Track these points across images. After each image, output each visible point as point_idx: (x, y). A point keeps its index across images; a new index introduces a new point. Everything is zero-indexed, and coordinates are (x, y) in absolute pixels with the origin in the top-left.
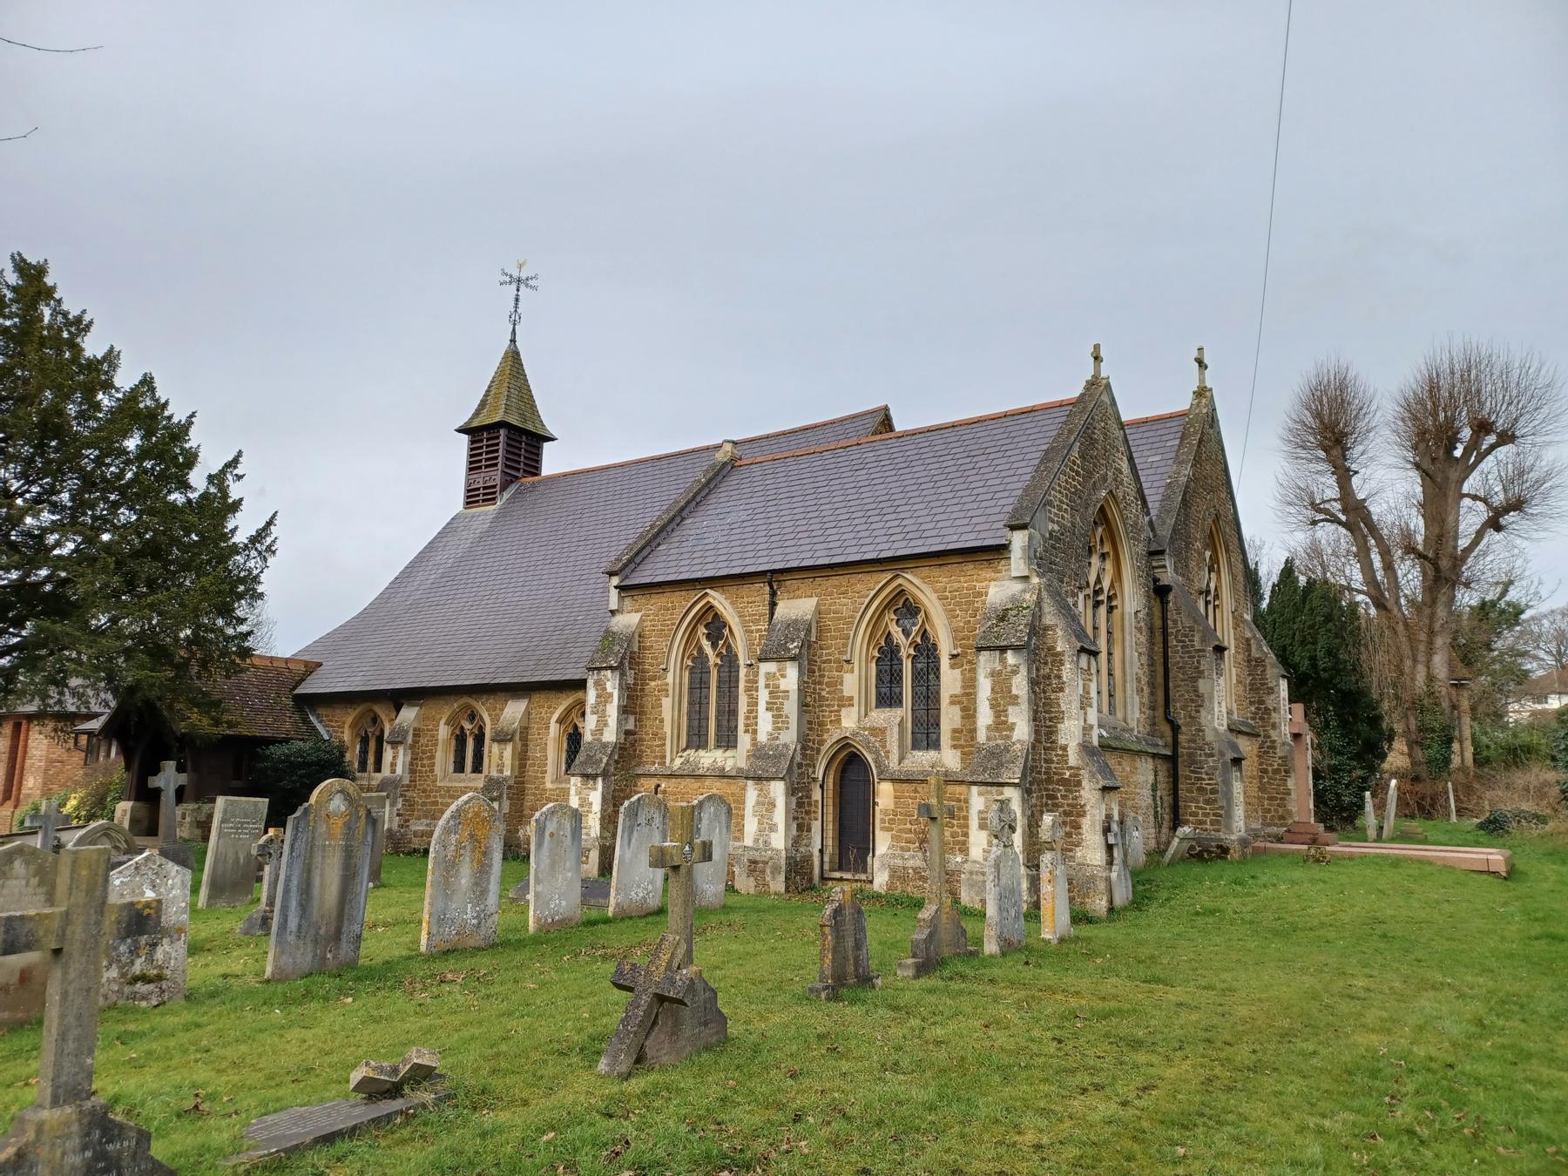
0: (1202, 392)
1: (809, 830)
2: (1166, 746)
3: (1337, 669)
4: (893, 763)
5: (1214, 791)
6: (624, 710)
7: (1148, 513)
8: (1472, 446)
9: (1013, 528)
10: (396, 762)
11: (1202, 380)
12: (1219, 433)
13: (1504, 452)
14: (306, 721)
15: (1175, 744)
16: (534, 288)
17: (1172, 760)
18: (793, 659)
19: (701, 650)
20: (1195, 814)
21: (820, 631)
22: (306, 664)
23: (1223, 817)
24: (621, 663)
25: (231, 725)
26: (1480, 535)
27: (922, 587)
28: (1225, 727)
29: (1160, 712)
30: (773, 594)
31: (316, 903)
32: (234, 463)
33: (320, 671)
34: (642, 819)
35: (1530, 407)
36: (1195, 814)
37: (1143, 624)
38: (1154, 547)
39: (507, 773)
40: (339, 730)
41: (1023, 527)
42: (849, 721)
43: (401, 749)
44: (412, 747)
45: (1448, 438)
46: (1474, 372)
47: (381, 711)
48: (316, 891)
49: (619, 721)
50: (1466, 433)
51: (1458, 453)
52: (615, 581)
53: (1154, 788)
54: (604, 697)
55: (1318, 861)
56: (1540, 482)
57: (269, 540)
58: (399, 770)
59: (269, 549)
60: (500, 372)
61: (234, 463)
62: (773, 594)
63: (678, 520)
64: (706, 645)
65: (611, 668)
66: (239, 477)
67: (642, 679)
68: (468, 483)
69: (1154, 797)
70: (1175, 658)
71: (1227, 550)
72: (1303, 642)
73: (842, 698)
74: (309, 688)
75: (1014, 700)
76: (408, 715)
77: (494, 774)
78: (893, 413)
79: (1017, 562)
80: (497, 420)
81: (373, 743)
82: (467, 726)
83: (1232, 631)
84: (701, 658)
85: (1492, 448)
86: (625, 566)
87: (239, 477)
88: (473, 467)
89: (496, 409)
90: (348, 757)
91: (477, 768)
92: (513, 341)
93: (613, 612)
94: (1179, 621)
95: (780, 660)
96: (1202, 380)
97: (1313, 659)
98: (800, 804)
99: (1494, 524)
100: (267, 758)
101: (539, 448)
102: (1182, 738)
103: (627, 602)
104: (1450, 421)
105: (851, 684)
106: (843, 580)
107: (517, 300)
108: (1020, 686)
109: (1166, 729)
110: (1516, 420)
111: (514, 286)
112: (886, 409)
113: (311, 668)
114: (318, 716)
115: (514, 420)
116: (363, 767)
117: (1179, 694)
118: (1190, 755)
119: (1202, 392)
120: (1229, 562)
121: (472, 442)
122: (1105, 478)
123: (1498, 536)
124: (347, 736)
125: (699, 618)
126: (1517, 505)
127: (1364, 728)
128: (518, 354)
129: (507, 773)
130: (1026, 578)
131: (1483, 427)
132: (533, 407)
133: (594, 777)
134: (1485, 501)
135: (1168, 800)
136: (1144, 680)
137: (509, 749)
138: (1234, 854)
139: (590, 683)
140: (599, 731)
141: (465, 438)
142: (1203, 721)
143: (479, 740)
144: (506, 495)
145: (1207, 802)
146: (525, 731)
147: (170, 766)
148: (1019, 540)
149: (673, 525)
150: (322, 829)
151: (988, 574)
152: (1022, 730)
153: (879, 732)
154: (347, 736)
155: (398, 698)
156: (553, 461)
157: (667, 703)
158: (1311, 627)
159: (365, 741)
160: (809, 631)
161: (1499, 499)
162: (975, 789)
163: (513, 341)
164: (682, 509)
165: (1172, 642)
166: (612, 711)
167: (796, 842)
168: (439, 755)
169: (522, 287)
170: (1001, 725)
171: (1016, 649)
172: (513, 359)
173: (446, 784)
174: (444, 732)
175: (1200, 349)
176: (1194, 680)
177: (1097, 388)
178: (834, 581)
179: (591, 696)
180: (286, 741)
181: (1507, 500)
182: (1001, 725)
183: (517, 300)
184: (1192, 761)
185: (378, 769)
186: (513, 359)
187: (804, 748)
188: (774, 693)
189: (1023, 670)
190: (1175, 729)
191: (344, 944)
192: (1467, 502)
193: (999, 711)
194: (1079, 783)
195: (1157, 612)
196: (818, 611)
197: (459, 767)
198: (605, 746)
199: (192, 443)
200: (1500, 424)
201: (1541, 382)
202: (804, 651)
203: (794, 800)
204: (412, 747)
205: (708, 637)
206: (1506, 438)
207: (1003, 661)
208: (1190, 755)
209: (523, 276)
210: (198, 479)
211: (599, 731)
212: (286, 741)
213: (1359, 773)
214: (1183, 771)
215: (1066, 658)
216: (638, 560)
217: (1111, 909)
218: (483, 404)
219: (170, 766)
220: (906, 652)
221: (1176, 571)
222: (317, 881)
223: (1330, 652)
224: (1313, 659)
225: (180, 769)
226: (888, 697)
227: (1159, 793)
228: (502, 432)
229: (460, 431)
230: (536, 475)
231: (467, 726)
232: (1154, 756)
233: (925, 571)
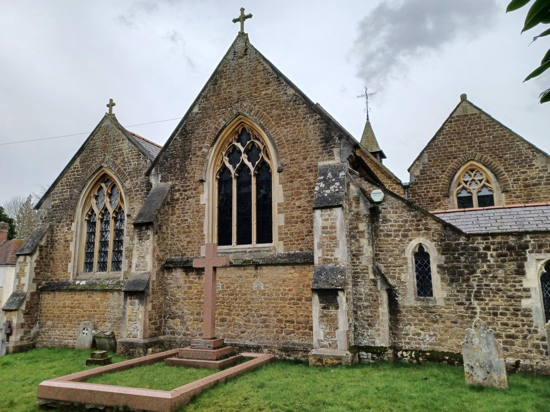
92: (368, 119)
163: (368, 119)
186: (368, 125)
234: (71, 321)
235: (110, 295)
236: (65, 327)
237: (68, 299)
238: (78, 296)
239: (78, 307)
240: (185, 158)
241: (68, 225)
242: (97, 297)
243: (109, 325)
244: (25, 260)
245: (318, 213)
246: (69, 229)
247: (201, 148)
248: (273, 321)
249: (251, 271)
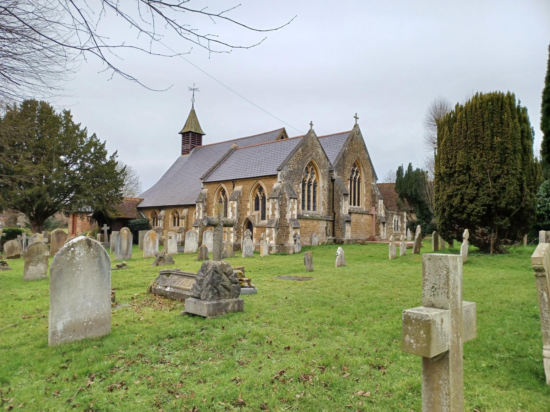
0: (356, 126)
1: (240, 238)
2: (332, 218)
3: (417, 195)
4: (256, 223)
5: (342, 228)
6: (204, 212)
7: (329, 161)
9: (278, 171)
10: (160, 223)
11: (356, 122)
12: (362, 136)
14: (140, 214)
15: (334, 217)
16: (199, 91)
17: (333, 221)
18: (236, 200)
19: (221, 197)
20: (338, 234)
21: (243, 193)
22: (140, 199)
23: (343, 234)
24: (203, 201)
25: (119, 215)
27: (262, 183)
28: (347, 212)
29: (331, 210)
30: (234, 185)
31: (122, 249)
32: (116, 153)
33: (143, 201)
34: (191, 235)
36: (338, 234)
37: (326, 189)
38: (331, 170)
39: (184, 226)
40: (147, 216)
41: (280, 170)
42: (249, 214)
43: (161, 220)
44: (163, 220)
47: (157, 211)
48: (122, 246)
49: (203, 214)
52: (202, 181)
53: (326, 228)
54: (199, 209)
55: (363, 244)
57: (125, 171)
58: (161, 226)
59: (125, 174)
60: (190, 116)
61: (116, 153)
62: (234, 185)
63: (219, 165)
64: (222, 196)
65: (201, 202)
66: (117, 156)
67: (209, 204)
68: (182, 148)
69: (326, 230)
70: (335, 197)
71: (363, 167)
72: (410, 187)
73: (247, 209)
74: (141, 205)
75: (275, 209)
76: (162, 212)
77: (181, 227)
78: (286, 130)
79: (279, 179)
80: (188, 131)
81: (156, 218)
82: (176, 215)
83: (364, 188)
84: (221, 199)
86: (205, 177)
87: (117, 156)
88: (183, 143)
89: (188, 127)
90: (150, 222)
91: (178, 225)
92: (193, 107)
93: (202, 188)
94: (336, 188)
95: (233, 200)
96: (356, 122)
97: (411, 192)
98: (237, 232)
100: (130, 223)
101: (201, 137)
102: (336, 216)
103: (205, 186)
105: (249, 205)
106: (247, 182)
107: (193, 95)
108: (277, 206)
109: (333, 214)
111: (192, 91)
112: (284, 128)
113: (141, 200)
114: (143, 213)
115: (193, 130)
116: (154, 225)
117: (336, 205)
118: (338, 220)
119: (356, 126)
120: (364, 170)
121: (183, 137)
122: (312, 155)
124: (149, 217)
125: (220, 190)
127: (425, 211)
128: (194, 111)
129: (184, 226)
130: (281, 182)
132: (199, 126)
133: (197, 227)
135: (331, 231)
136: (326, 203)
137: (184, 220)
138: (345, 243)
139: (197, 205)
140: (199, 216)
141: (181, 135)
142: (340, 212)
143: (178, 218)
144: (192, 151)
145: (340, 231)
146: (187, 216)
147: (105, 225)
148: (279, 173)
149: (218, 166)
150: (123, 236)
151: (274, 181)
152: (277, 216)
153: (254, 216)
154: (149, 217)
155: (160, 208)
156: (205, 141)
157: (213, 210)
158: (412, 183)
159: (154, 219)
160: (240, 193)
162: (267, 228)
163: (193, 107)
164: (220, 162)
165: (335, 193)
166: (201, 212)
167: (236, 241)
168: (170, 222)
169: (195, 91)
170: (273, 215)
171: (276, 198)
172: (193, 112)
173: (171, 229)
174: (171, 216)
175: (356, 114)
176: (339, 202)
177: (311, 131)
178: (246, 182)
179: (197, 208)
180: (135, 219)
182: (273, 215)
183: (193, 95)
184: (338, 222)
185: (157, 226)
186: (193, 112)
187: (239, 220)
188: (233, 208)
189: (277, 203)
190: (335, 214)
191: (128, 255)
193: (273, 212)
194: (289, 227)
195: (332, 185)
196: (243, 189)
197: (174, 225)
198: (200, 220)
199: (105, 149)
202: (239, 198)
203: (236, 231)
204: (163, 220)
205: (222, 194)
207: (274, 200)
208: (338, 220)
209: (195, 88)
210: (108, 158)
211: (199, 216)
212: (135, 219)
213: (424, 223)
214: (336, 224)
215: (288, 200)
216: (208, 175)
217: (294, 253)
218: (185, 126)
219: (105, 225)
220: (260, 198)
221: (338, 175)
222: (122, 245)
223: (416, 190)
224: (411, 192)
225: (107, 226)
226: (257, 209)
227: (328, 229)
228: (190, 134)
229: (179, 133)
230: (201, 145)
231: (176, 215)
232: (326, 220)
233: (263, 180)
234: (305, 234)
235: (320, 222)
236: (303, 237)
237: (303, 223)
238: (308, 222)
239: (308, 227)
240: (344, 168)
241: (298, 184)
242: (315, 223)
243: (320, 235)
244: (294, 202)
245: (379, 200)
246: (299, 186)
247: (348, 166)
248: (365, 232)
249: (361, 216)
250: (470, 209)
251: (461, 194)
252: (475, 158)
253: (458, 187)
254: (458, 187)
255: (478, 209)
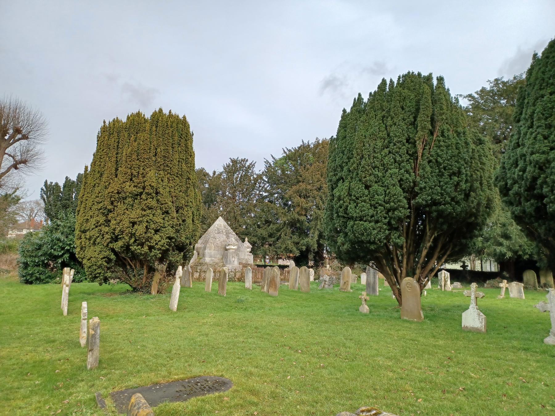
8: (12, 137)
13: (23, 142)
26: (9, 170)
35: (35, 129)
45: (4, 131)
46: (18, 111)
50: (11, 131)
51: (6, 138)
56: (33, 156)
85: (19, 139)
99: (15, 167)
104: (5, 125)
110: (30, 132)
123: (15, 171)
126: (24, 162)
131: (17, 131)
134: (13, 157)
161: (18, 158)
181: (21, 159)
192: (6, 156)
200: (24, 132)
201: (40, 122)
206: (25, 137)
250: (156, 241)
251: (147, 222)
252: (162, 180)
253: (144, 213)
254: (144, 213)
255: (163, 241)
